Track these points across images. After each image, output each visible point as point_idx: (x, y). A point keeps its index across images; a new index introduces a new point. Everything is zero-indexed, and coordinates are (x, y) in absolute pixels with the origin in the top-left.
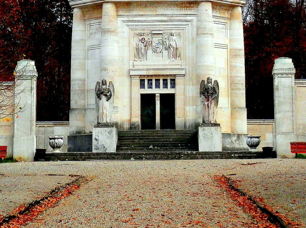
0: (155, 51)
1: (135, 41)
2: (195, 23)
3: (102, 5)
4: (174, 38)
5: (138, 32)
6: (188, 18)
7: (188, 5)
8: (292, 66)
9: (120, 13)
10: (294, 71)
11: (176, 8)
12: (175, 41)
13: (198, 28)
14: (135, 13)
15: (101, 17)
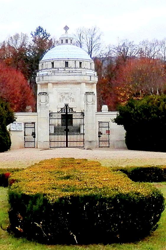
0: (66, 100)
1: (59, 96)
2: (80, 90)
3: (48, 84)
4: (72, 95)
5: (60, 93)
6: (78, 88)
7: (77, 83)
8: (107, 108)
9: (54, 86)
10: (108, 109)
11: (73, 85)
12: (73, 96)
13: (81, 92)
14: (59, 86)
15: (47, 88)
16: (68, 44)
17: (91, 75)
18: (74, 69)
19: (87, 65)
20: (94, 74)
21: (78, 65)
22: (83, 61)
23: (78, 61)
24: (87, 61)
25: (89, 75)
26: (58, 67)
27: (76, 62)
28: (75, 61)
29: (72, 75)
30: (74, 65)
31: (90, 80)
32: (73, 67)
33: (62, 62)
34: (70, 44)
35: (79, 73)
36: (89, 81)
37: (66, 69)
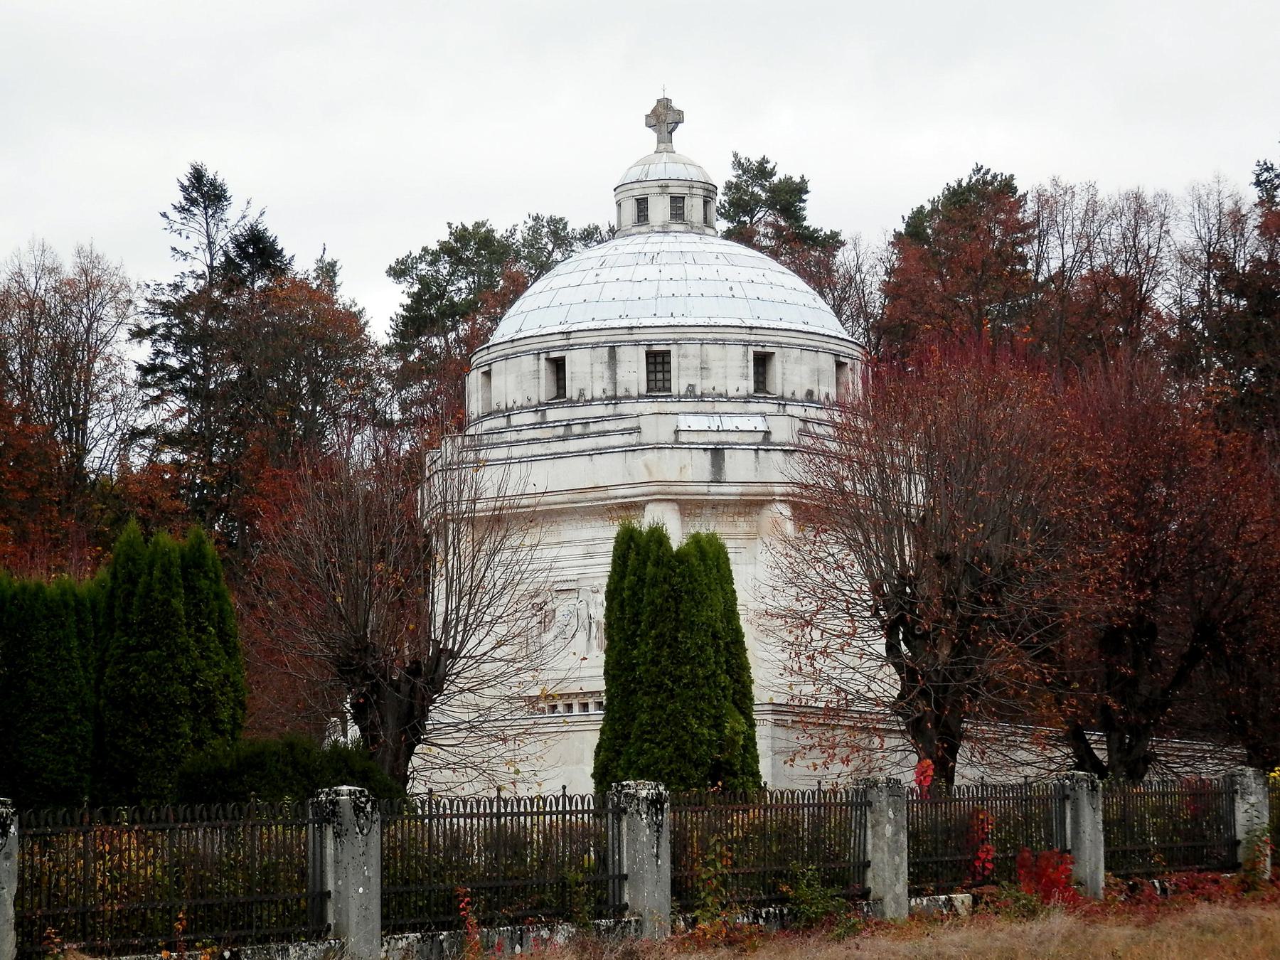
11: (600, 523)
16: (653, 231)
17: (724, 437)
18: (599, 410)
19: (715, 366)
20: (762, 427)
21: (633, 371)
22: (676, 342)
23: (637, 343)
24: (715, 342)
25: (715, 438)
26: (510, 406)
27: (624, 353)
28: (612, 350)
29: (580, 453)
30: (607, 374)
31: (717, 481)
32: (598, 393)
33: (528, 361)
34: (665, 231)
35: (622, 432)
36: (704, 489)
37: (552, 415)
